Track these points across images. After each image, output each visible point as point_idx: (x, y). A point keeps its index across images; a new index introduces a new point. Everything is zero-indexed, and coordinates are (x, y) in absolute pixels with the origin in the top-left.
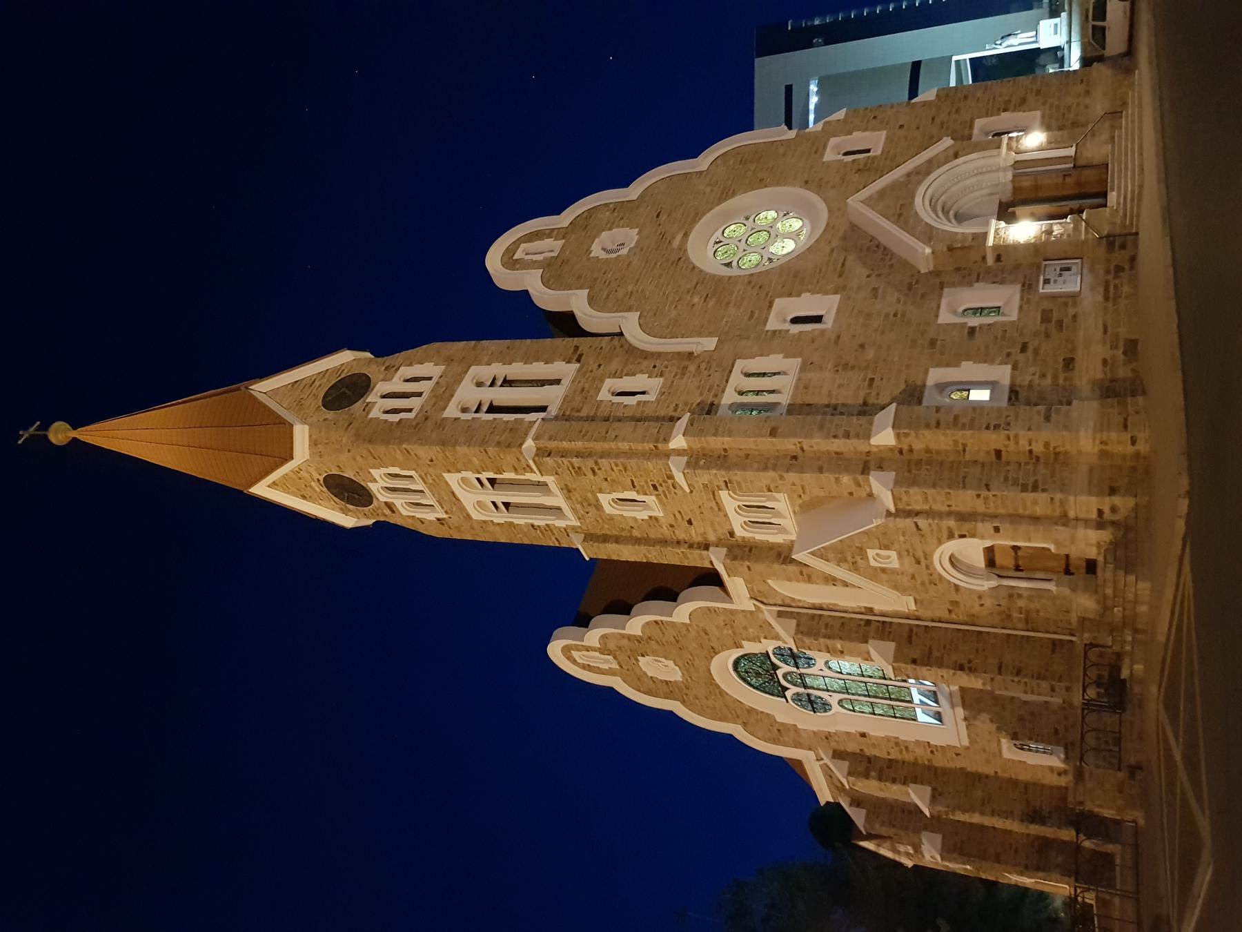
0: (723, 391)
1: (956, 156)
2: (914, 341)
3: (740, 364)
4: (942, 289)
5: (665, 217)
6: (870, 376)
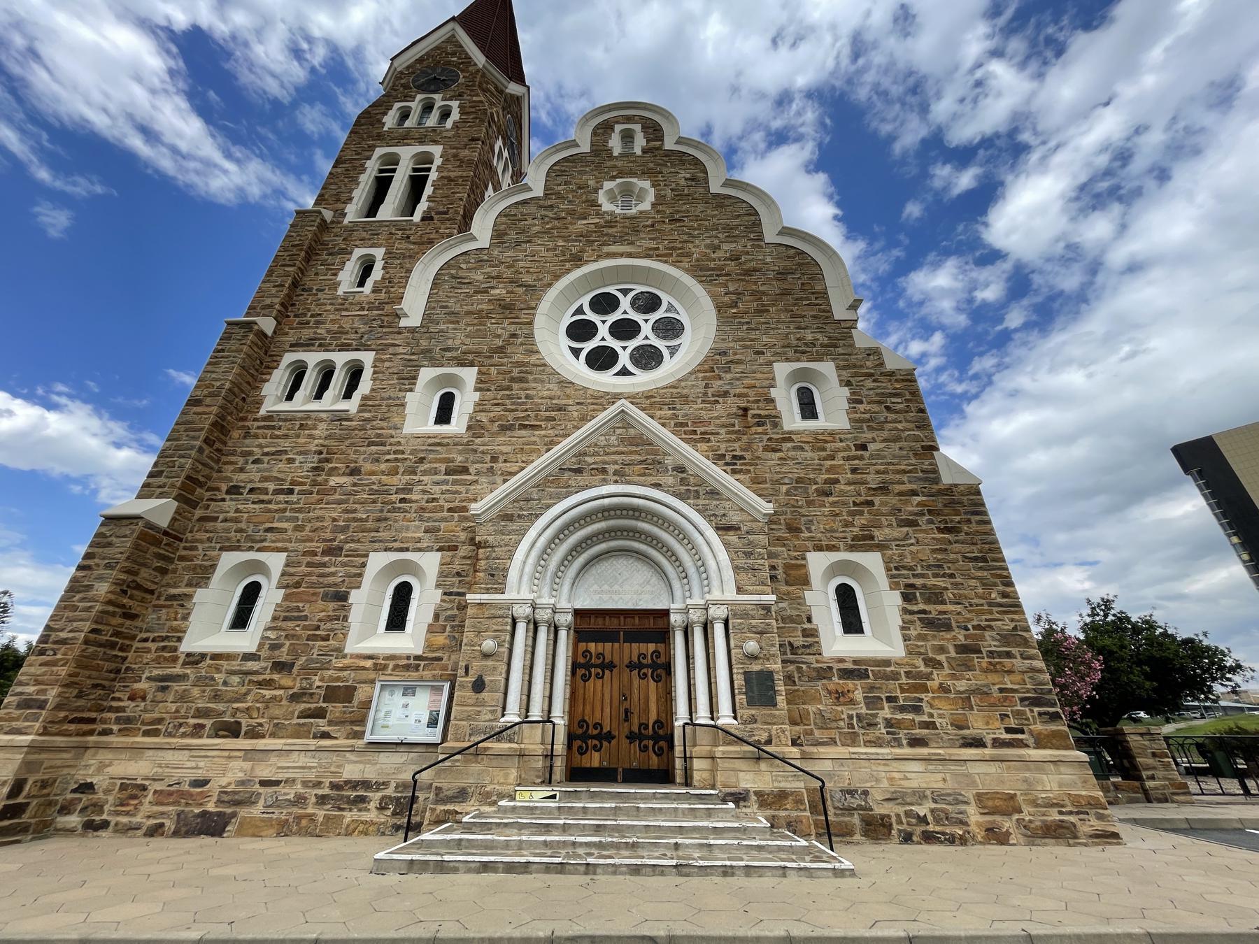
0: (327, 350)
1: (723, 529)
2: (344, 530)
3: (367, 358)
4: (438, 550)
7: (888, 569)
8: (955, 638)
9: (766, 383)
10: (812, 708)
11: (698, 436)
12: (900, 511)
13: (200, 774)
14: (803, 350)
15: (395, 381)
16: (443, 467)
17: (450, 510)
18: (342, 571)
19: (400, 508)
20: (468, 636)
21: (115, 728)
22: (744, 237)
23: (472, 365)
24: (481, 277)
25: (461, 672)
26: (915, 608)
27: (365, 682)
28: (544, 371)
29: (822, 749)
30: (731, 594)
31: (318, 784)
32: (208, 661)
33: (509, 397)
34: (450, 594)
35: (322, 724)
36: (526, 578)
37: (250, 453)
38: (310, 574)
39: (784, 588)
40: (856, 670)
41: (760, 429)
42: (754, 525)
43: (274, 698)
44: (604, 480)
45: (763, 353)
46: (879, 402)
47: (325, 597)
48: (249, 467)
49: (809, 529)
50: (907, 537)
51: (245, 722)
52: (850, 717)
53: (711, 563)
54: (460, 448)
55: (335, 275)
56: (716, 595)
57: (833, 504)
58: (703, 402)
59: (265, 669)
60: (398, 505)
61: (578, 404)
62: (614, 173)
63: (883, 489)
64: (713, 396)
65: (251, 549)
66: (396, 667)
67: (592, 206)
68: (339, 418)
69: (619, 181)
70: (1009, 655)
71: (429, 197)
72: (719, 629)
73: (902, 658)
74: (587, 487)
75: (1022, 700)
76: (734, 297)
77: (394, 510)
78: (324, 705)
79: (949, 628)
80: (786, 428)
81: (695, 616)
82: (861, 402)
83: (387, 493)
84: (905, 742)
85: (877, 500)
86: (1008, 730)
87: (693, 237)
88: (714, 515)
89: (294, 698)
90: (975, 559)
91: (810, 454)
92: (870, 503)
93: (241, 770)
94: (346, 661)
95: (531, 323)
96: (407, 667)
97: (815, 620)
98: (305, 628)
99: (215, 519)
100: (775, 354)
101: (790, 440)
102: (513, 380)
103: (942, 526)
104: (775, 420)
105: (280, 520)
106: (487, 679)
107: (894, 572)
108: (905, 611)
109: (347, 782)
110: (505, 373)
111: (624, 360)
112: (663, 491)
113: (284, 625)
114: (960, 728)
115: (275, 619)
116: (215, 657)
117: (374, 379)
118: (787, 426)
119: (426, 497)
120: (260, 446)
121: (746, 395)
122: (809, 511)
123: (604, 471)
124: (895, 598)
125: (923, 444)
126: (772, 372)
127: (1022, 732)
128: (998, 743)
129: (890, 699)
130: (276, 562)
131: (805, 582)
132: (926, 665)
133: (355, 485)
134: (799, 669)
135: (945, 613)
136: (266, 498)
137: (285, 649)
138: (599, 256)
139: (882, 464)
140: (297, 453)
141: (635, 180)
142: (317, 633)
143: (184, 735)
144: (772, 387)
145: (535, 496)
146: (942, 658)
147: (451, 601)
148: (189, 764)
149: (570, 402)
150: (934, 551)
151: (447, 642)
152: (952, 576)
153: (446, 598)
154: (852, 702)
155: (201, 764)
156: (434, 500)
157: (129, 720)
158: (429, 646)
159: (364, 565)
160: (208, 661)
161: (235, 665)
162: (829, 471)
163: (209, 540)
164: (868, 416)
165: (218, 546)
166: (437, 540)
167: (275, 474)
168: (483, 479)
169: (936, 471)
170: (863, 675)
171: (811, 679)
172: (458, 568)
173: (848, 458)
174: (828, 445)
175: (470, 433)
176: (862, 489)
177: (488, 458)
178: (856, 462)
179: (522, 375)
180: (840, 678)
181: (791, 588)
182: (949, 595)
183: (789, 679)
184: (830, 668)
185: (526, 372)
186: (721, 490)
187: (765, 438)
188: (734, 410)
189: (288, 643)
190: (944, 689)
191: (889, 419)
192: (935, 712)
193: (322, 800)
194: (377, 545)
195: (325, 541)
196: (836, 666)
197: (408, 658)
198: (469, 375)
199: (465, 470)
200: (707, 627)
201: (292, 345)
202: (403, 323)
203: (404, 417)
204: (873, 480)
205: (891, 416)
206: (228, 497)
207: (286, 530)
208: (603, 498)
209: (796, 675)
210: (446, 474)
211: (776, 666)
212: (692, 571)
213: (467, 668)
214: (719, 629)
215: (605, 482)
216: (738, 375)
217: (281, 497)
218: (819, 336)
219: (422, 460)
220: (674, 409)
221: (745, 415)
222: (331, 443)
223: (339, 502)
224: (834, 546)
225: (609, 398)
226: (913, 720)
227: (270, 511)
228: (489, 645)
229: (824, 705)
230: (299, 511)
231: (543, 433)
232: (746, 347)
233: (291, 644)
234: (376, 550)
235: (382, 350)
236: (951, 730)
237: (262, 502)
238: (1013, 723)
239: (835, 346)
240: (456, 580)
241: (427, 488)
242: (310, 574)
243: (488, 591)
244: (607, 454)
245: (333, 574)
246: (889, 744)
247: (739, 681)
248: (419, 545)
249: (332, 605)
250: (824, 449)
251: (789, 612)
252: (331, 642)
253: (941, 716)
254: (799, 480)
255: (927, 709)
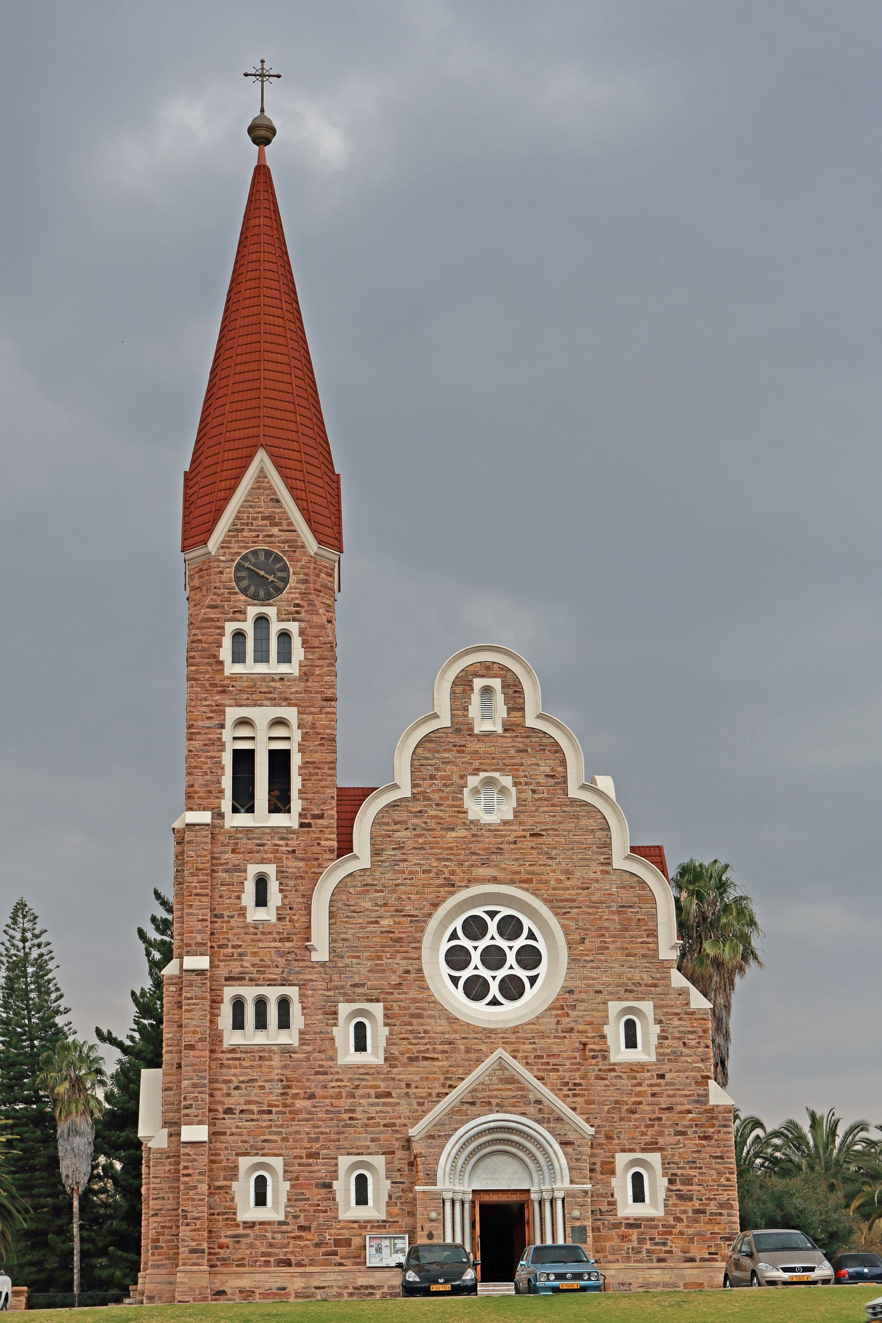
0: (257, 985)
1: (564, 1144)
2: (317, 1140)
3: (293, 992)
4: (382, 1154)
5: (530, 844)
6: (274, 1109)
7: (663, 1164)
8: (693, 1205)
9: (601, 1021)
10: (608, 1244)
11: (551, 1067)
12: (677, 1124)
13: (280, 1285)
14: (631, 991)
15: (320, 1017)
16: (372, 1092)
17: (384, 1125)
18: (324, 1169)
19: (350, 1124)
20: (420, 1209)
21: (219, 1263)
22: (594, 860)
23: (378, 1000)
24: (368, 905)
25: (419, 1229)
26: (674, 1188)
27: (356, 1236)
28: (434, 1007)
29: (611, 1264)
30: (567, 1185)
31: (347, 1287)
32: (258, 1226)
33: (411, 1032)
34: (396, 1183)
35: (337, 1259)
36: (447, 1176)
37: (230, 1081)
38: (303, 1171)
39: (600, 1176)
40: (635, 1224)
41: (594, 1061)
42: (583, 1141)
43: (306, 1246)
44: (491, 1110)
45: (601, 992)
46: (679, 1038)
47: (317, 1186)
48: (234, 1092)
49: (619, 1138)
50: (678, 1142)
51: (292, 1258)
52: (628, 1249)
53: (556, 1165)
54: (382, 1076)
55: (239, 898)
56: (559, 1185)
57: (636, 1120)
58: (555, 1037)
59: (295, 1230)
60: (349, 1122)
61: (463, 1038)
62: (476, 764)
63: (670, 1109)
64: (562, 1032)
65: (257, 1154)
66: (372, 1227)
67: (459, 812)
68: (286, 1051)
69: (483, 775)
70: (721, 1214)
71: (300, 792)
72: (559, 1204)
73: (661, 1217)
74: (479, 1115)
75: (721, 1238)
76: (583, 932)
77: (347, 1126)
78: (336, 1249)
79: (691, 1199)
80: (612, 1060)
81: (546, 1196)
82: (666, 1038)
83: (339, 1112)
84: (655, 1260)
85: (664, 1116)
86: (710, 1254)
87: (551, 858)
88: (559, 1135)
89: (317, 1245)
90: (717, 1157)
91: (625, 1082)
92: (660, 1119)
93: (301, 1282)
94: (342, 1224)
95: (419, 958)
96: (379, 1227)
97: (615, 1196)
98: (310, 1205)
99: (225, 1134)
100: (611, 993)
101: (613, 1070)
102: (412, 1016)
103: (702, 1135)
104: (604, 1054)
105: (270, 1133)
106: (433, 1232)
107: (667, 1166)
108: (669, 1190)
109: (362, 1286)
110: (405, 1009)
111: (494, 990)
112: (527, 1118)
113: (297, 1203)
114: (685, 1253)
115: (289, 1200)
116: (261, 1223)
117: (304, 1015)
118: (614, 1058)
119: (366, 1116)
120: (235, 1075)
121: (586, 1032)
122: (620, 1125)
123: (489, 1103)
124: (665, 1182)
125: (703, 1074)
126: (606, 1010)
127: (717, 1254)
128: (703, 1260)
129: (651, 1239)
130: (277, 1163)
131: (613, 1172)
132: (674, 1220)
133: (315, 1107)
134: (603, 1223)
135: (691, 1191)
136: (252, 1117)
137: (302, 1218)
138: (469, 881)
139: (672, 1090)
140: (265, 1081)
141: (496, 775)
142: (319, 1208)
143: (260, 1266)
144: (606, 1024)
145: (447, 1122)
146: (684, 1217)
147: (398, 1187)
148: (271, 1280)
149: (458, 1036)
150: (692, 1152)
151: (400, 1212)
152: (701, 1168)
153: (394, 1185)
154: (630, 1241)
155: (278, 1280)
156: (372, 1118)
157: (224, 1259)
158: (389, 1213)
159: (336, 1165)
160: (258, 1226)
161: (276, 1227)
162: (637, 1095)
163: (226, 1148)
164: (668, 1051)
165: (234, 1153)
166: (381, 1146)
167: (255, 1099)
168: (403, 1102)
169: (707, 1096)
170: (638, 1226)
171: (609, 1229)
172: (398, 1166)
173: (651, 1085)
174: (638, 1075)
175: (388, 1064)
176: (657, 1107)
177: (403, 1085)
178: (656, 1088)
179: (419, 1011)
180: (626, 1228)
181: (603, 1177)
182: (696, 1180)
183: (595, 1229)
184: (621, 1223)
185: (421, 1009)
186: (564, 1117)
187: (597, 1068)
188: (577, 1045)
189: (302, 1215)
190: (681, 1233)
191: (684, 1053)
192: (673, 1245)
193: (351, 1295)
194: (343, 1151)
195: (306, 1148)
196: (624, 1222)
197: (378, 1221)
198: (377, 1009)
199: (389, 1095)
200: (552, 1201)
201: (227, 979)
202: (315, 957)
203: (335, 1050)
204: (664, 1102)
205: (686, 1051)
206: (226, 1116)
207: (275, 1141)
208: (490, 1122)
209: (601, 1227)
210: (376, 1097)
211: (588, 1223)
212: (545, 1168)
213: (422, 1227)
214: (559, 1204)
215: (491, 1112)
216: (581, 1013)
217: (265, 1117)
218: (645, 976)
219: (357, 1087)
220: (534, 1043)
221: (584, 1049)
222: (287, 1072)
223: (308, 1120)
224: (632, 1149)
225: (488, 1034)
226: (661, 1250)
227: (261, 1127)
228: (433, 1215)
229: (616, 1242)
230: (281, 1126)
231: (440, 1064)
232: (588, 985)
233: (305, 1215)
234: (342, 1155)
235: (304, 985)
236: (680, 1254)
237: (253, 1120)
238: (713, 1250)
239: (655, 986)
240: (398, 1174)
241: (366, 1108)
242: (303, 1171)
243: (427, 1184)
244: (491, 1090)
245: (318, 1171)
246: (646, 1261)
247: (569, 1231)
248: (369, 1151)
249: (323, 1191)
250: (636, 1078)
251: (601, 1191)
252: (329, 1213)
253: (676, 1247)
254: (617, 1102)
255: (669, 1244)
